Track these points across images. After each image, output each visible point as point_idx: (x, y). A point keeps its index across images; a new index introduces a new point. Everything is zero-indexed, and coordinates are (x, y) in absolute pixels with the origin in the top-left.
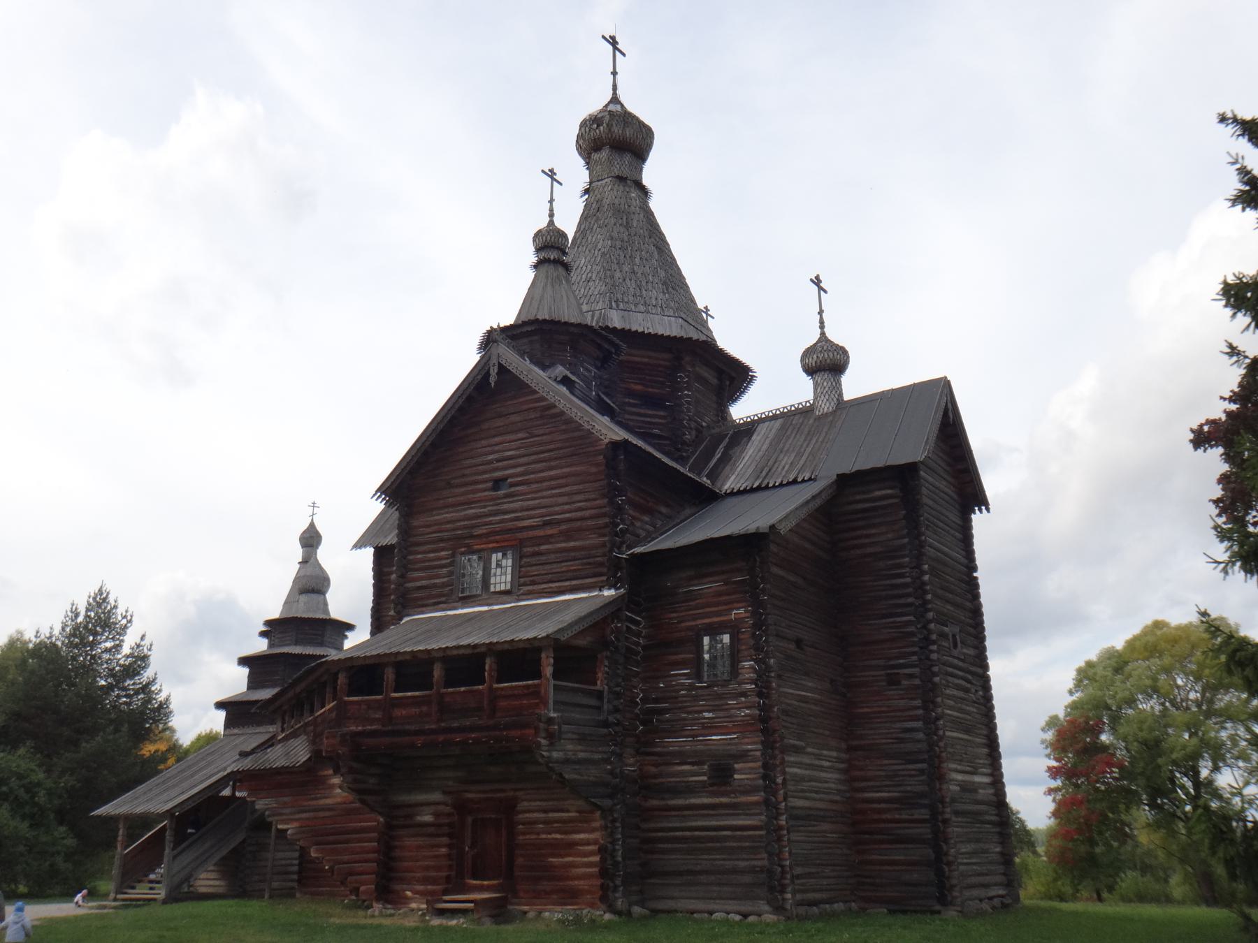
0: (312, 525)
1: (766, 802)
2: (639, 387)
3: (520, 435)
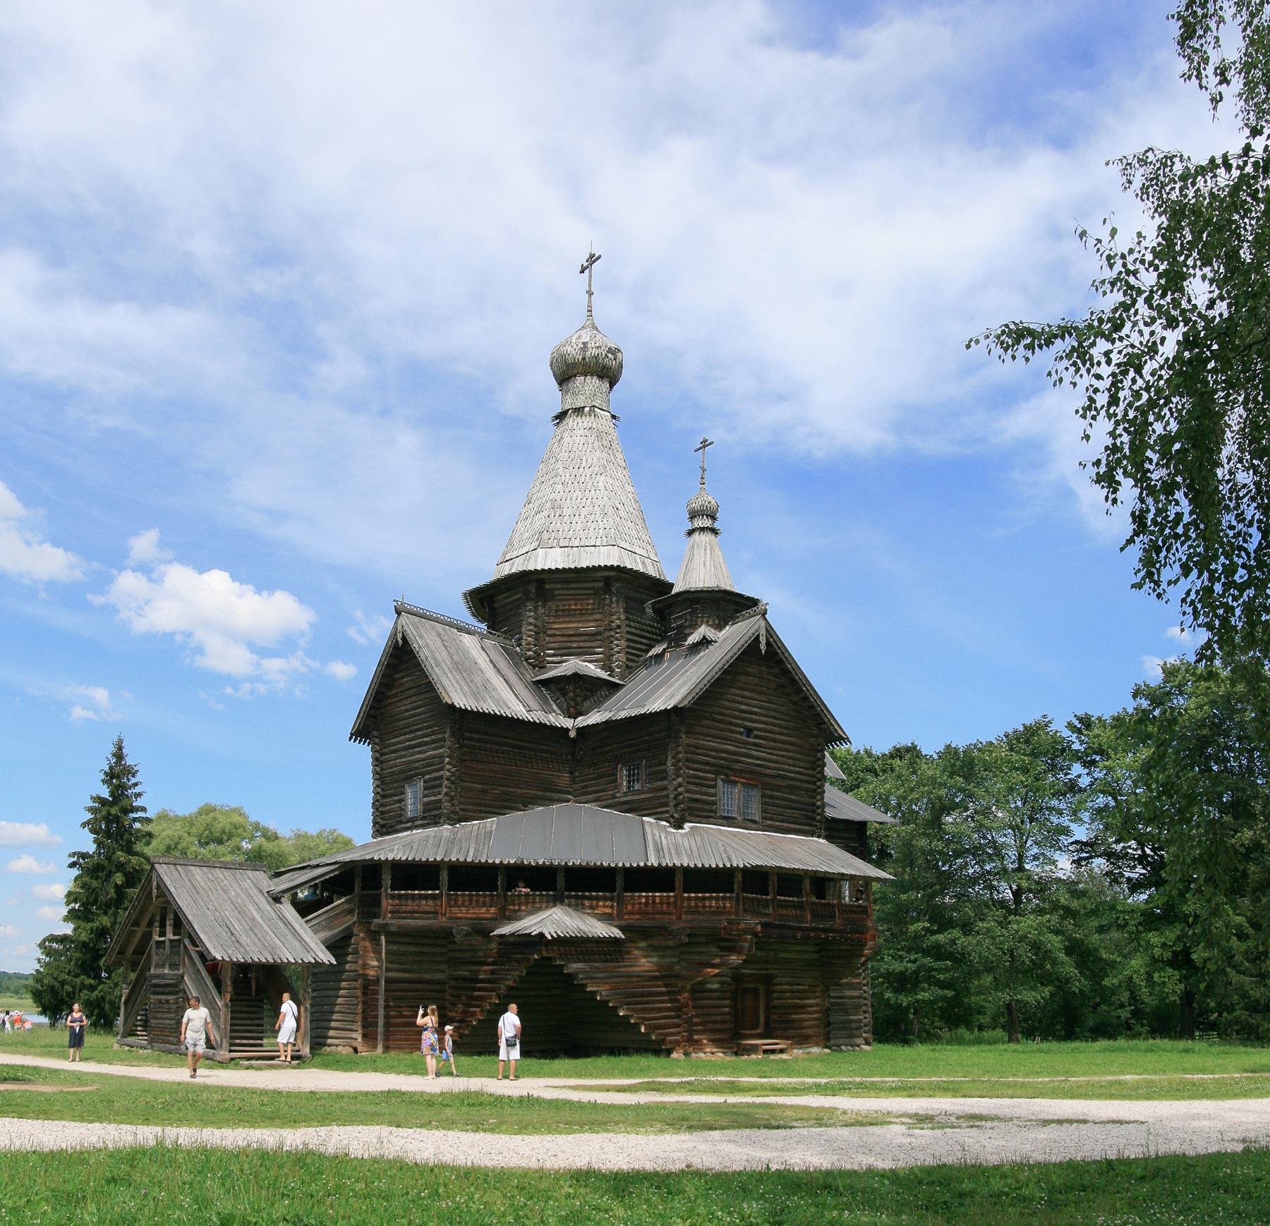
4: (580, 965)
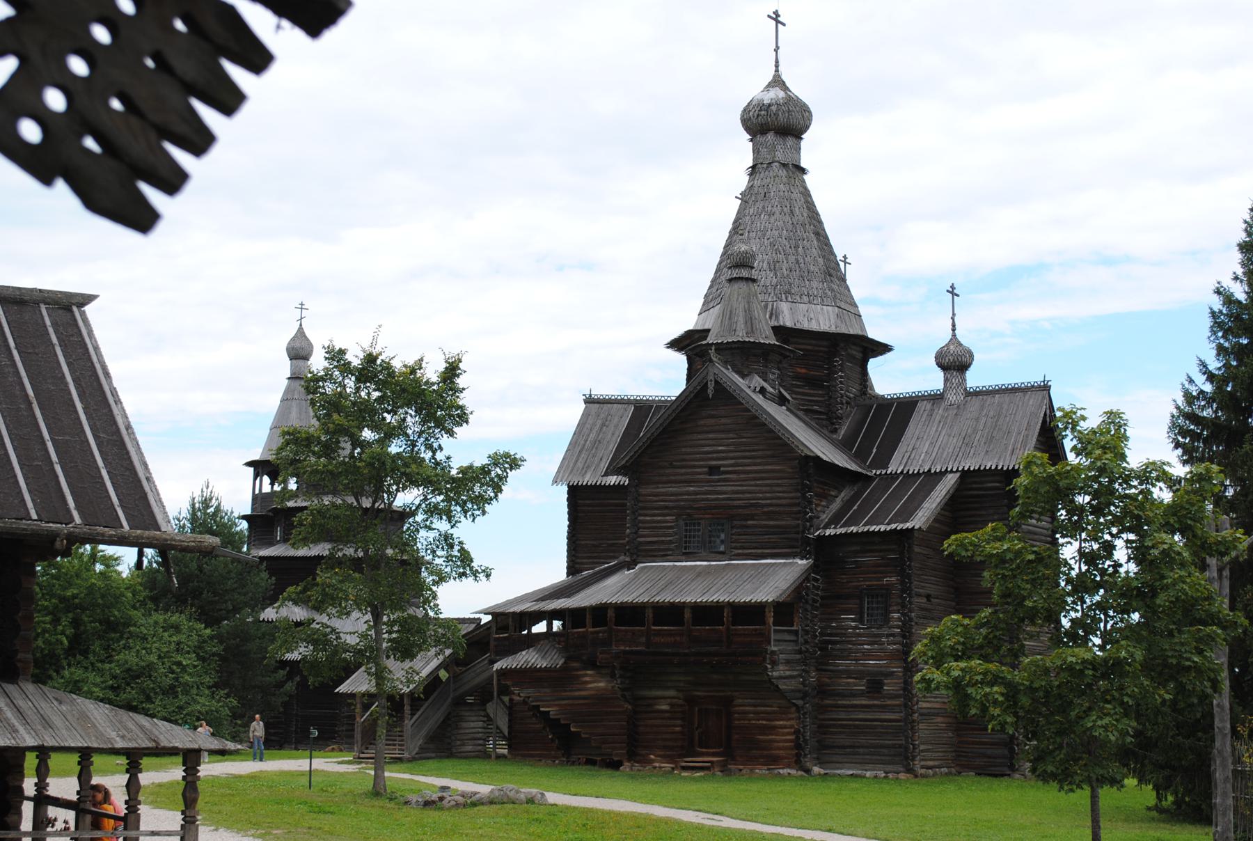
0: (301, 333)
1: (906, 706)
2: (803, 371)
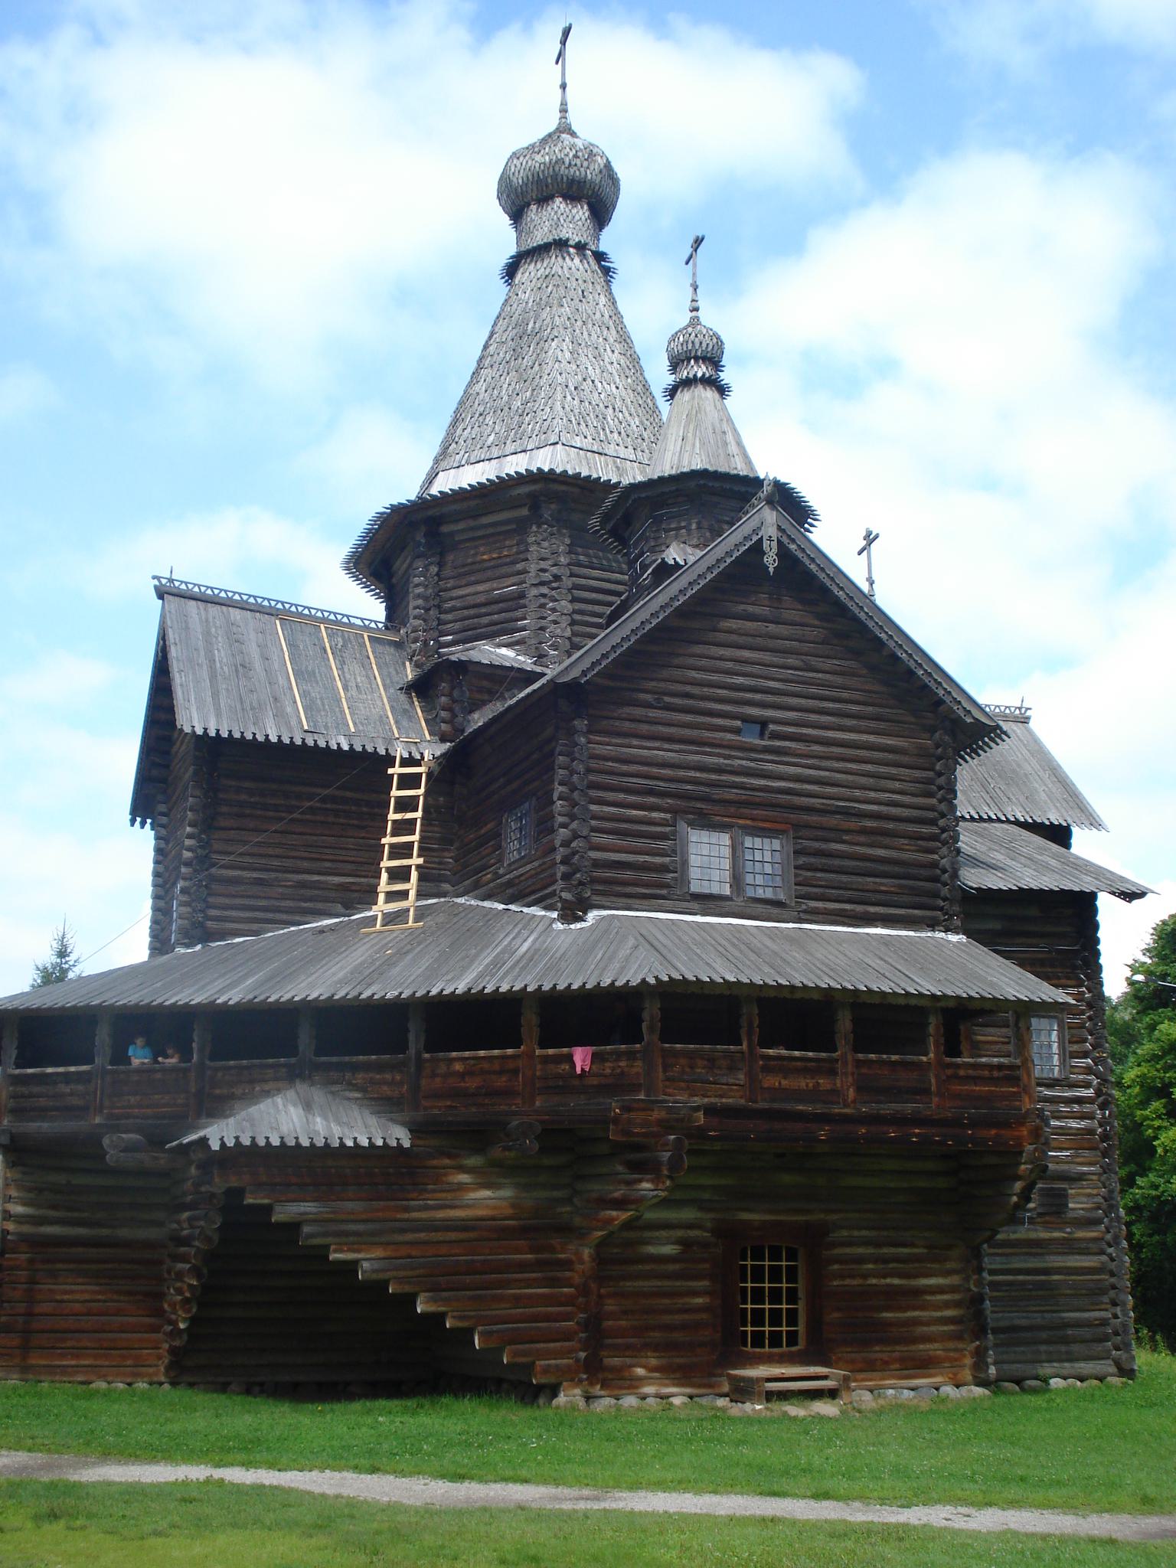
3: (791, 661)
4: (308, 1208)
